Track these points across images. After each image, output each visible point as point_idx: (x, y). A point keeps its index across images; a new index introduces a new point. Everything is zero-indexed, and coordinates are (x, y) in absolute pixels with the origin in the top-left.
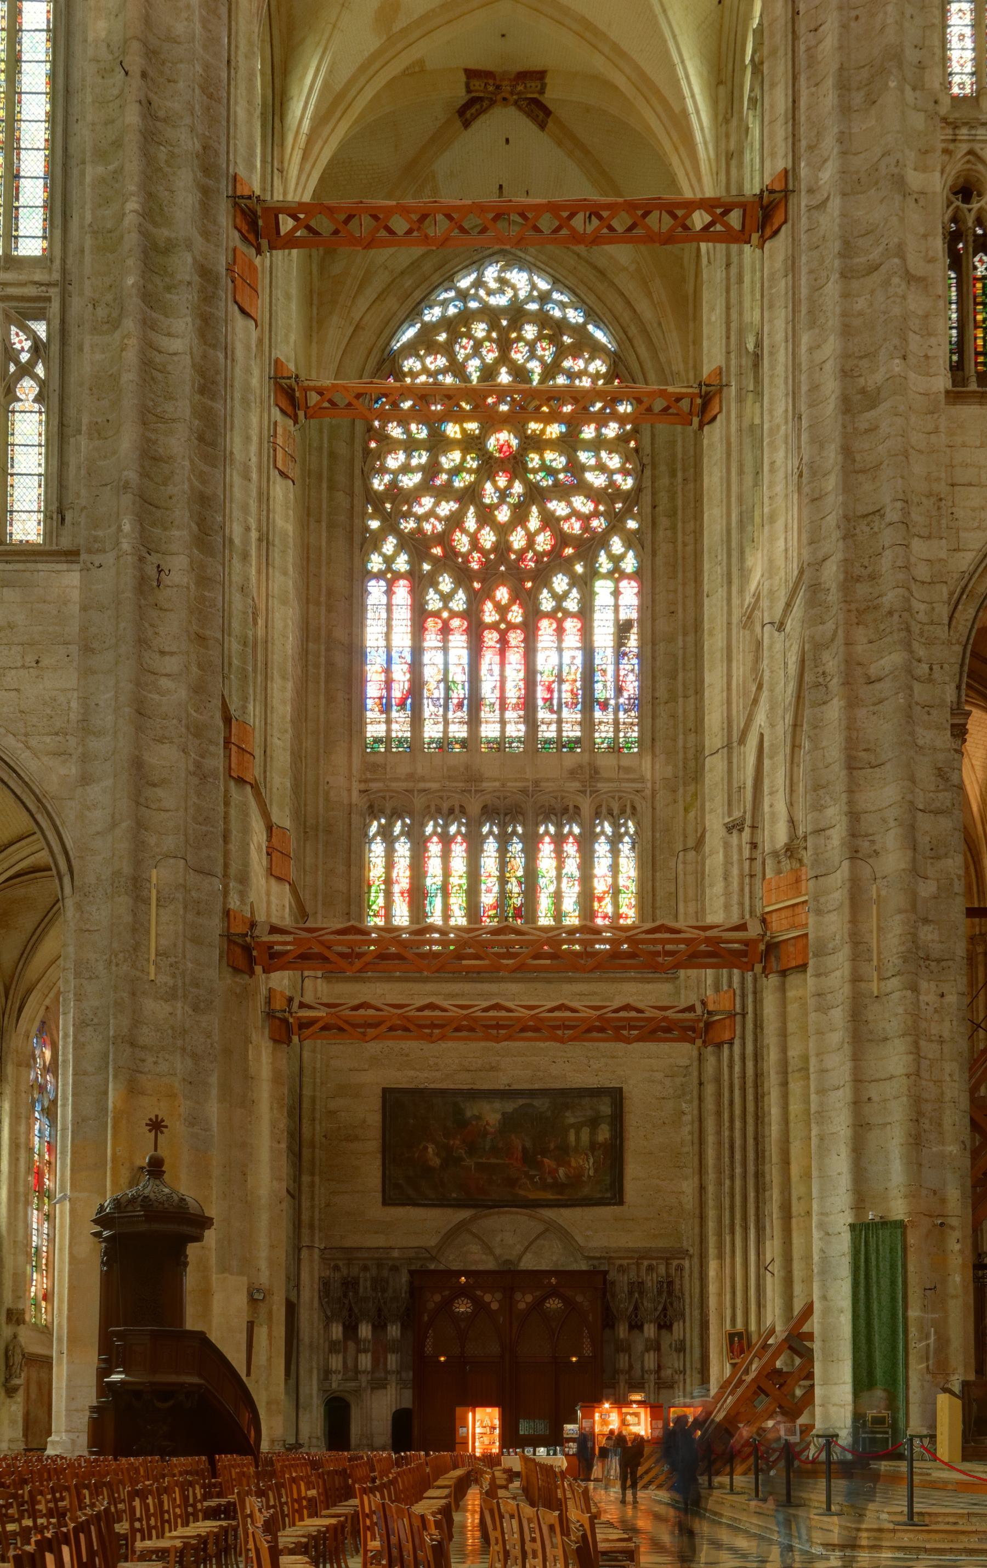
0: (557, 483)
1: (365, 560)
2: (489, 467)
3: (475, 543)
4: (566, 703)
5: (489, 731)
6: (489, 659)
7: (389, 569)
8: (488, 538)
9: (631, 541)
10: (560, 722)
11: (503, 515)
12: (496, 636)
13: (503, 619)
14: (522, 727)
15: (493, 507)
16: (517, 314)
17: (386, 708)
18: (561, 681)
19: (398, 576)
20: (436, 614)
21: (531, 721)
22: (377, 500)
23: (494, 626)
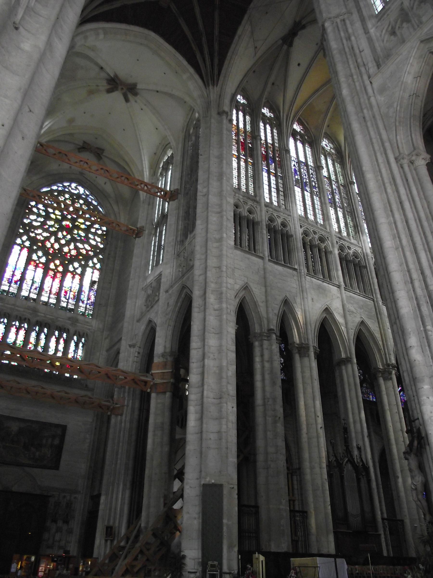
0: (81, 239)
1: (16, 239)
2: (61, 228)
3: (52, 245)
4: (71, 298)
5: (44, 298)
6: (48, 280)
7: (23, 244)
8: (57, 246)
9: (99, 260)
10: (68, 302)
11: (63, 242)
12: (53, 273)
13: (56, 269)
14: (55, 301)
15: (60, 239)
16: (79, 196)
17: (10, 282)
18: (71, 291)
19: (25, 247)
20: (35, 261)
21: (58, 299)
22: (25, 225)
23: (53, 270)
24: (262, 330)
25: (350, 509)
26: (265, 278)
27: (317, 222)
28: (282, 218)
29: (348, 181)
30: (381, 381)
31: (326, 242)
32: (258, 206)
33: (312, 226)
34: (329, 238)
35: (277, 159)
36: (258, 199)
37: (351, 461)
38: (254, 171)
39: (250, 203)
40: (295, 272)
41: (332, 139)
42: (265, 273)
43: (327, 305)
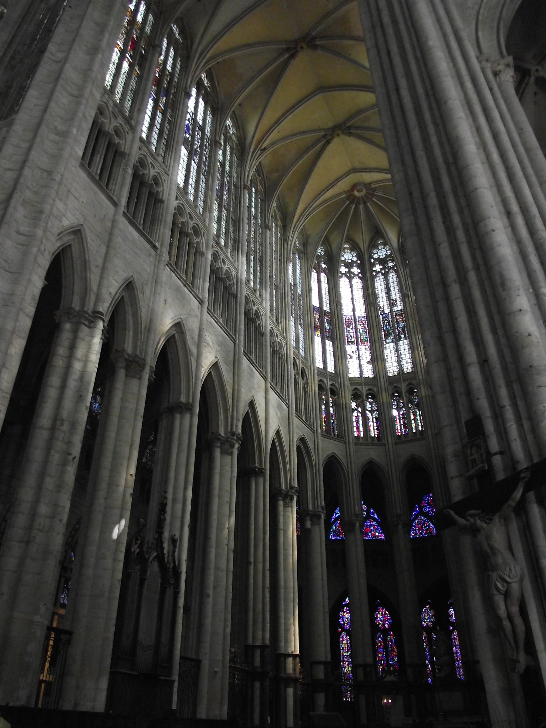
24: (83, 308)
25: (141, 636)
26: (111, 234)
27: (196, 206)
28: (156, 170)
29: (242, 182)
30: (217, 452)
31: (200, 238)
32: (130, 133)
33: (190, 205)
34: (205, 234)
35: (172, 96)
36: (133, 123)
37: (160, 558)
38: (138, 84)
39: (121, 120)
40: (152, 251)
41: (237, 124)
42: (113, 227)
43: (181, 318)
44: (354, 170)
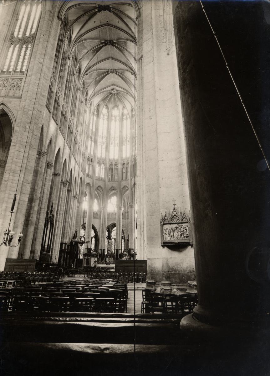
44: (113, 84)
